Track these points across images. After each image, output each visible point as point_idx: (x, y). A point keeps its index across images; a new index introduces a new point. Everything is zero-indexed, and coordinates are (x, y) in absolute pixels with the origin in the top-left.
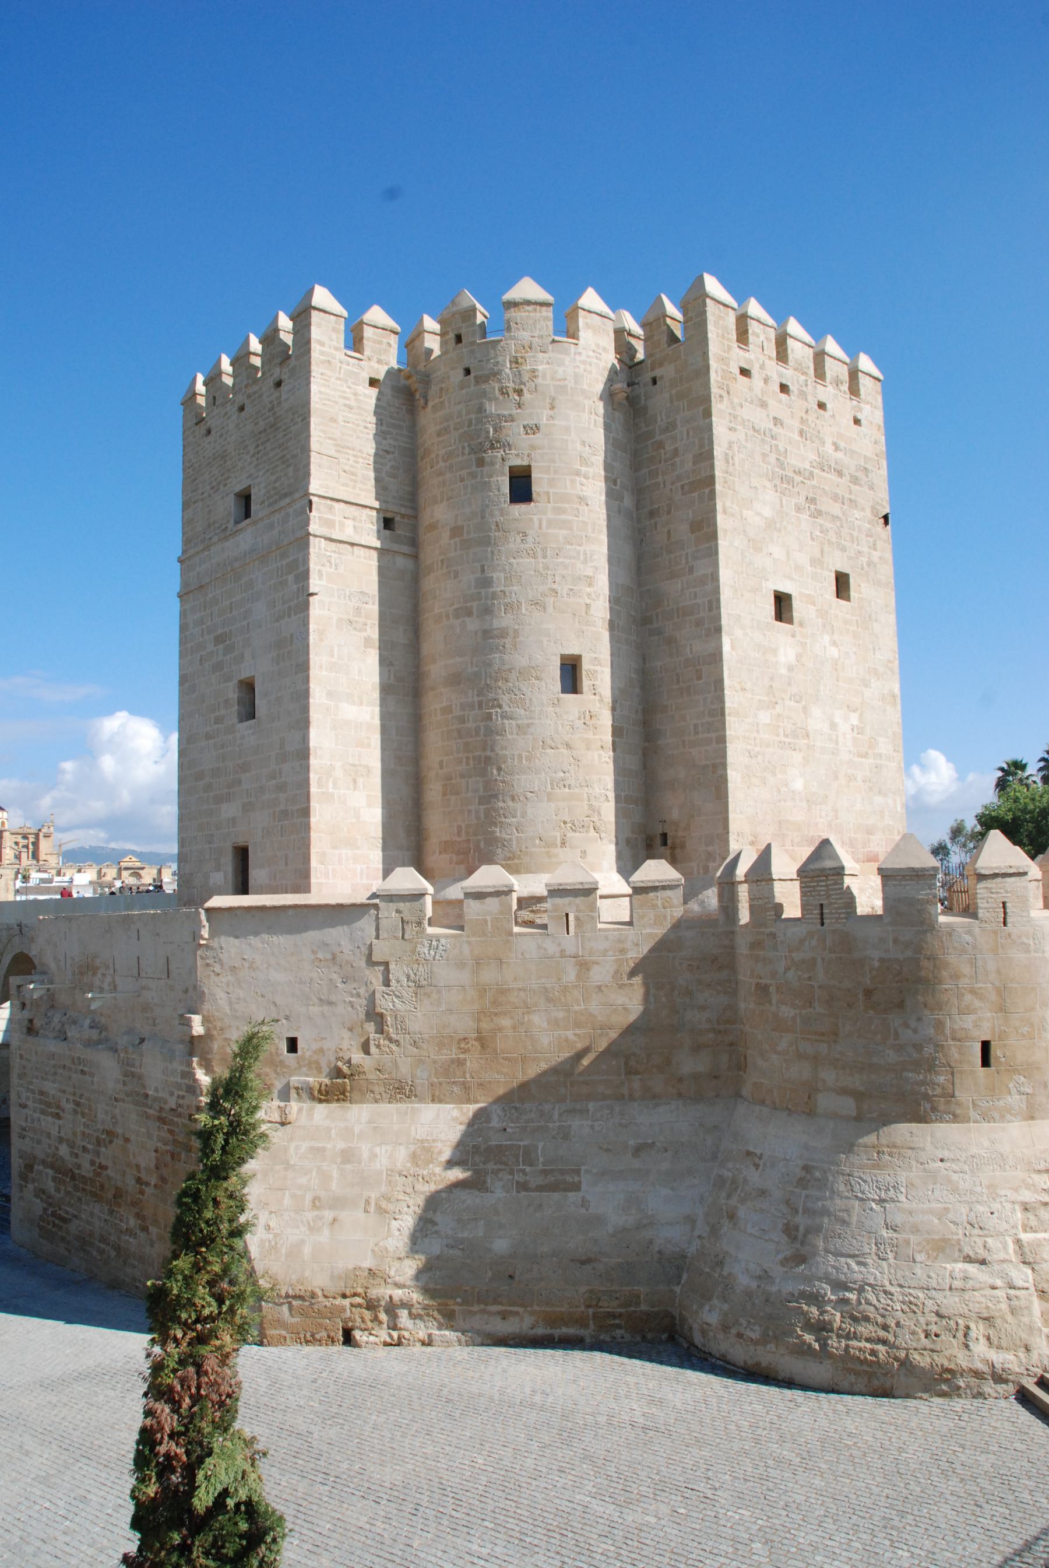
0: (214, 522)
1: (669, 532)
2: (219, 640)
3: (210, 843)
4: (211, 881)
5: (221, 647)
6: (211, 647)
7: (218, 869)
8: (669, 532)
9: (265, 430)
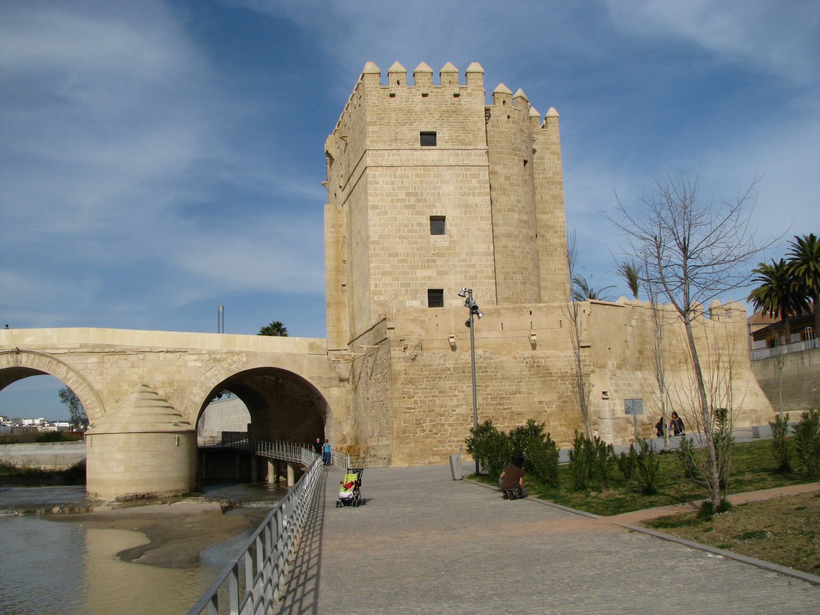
0: (401, 139)
1: (542, 196)
2: (408, 194)
3: (405, 287)
4: (408, 305)
5: (413, 199)
6: (404, 197)
7: (415, 298)
8: (542, 196)
9: (448, 112)
